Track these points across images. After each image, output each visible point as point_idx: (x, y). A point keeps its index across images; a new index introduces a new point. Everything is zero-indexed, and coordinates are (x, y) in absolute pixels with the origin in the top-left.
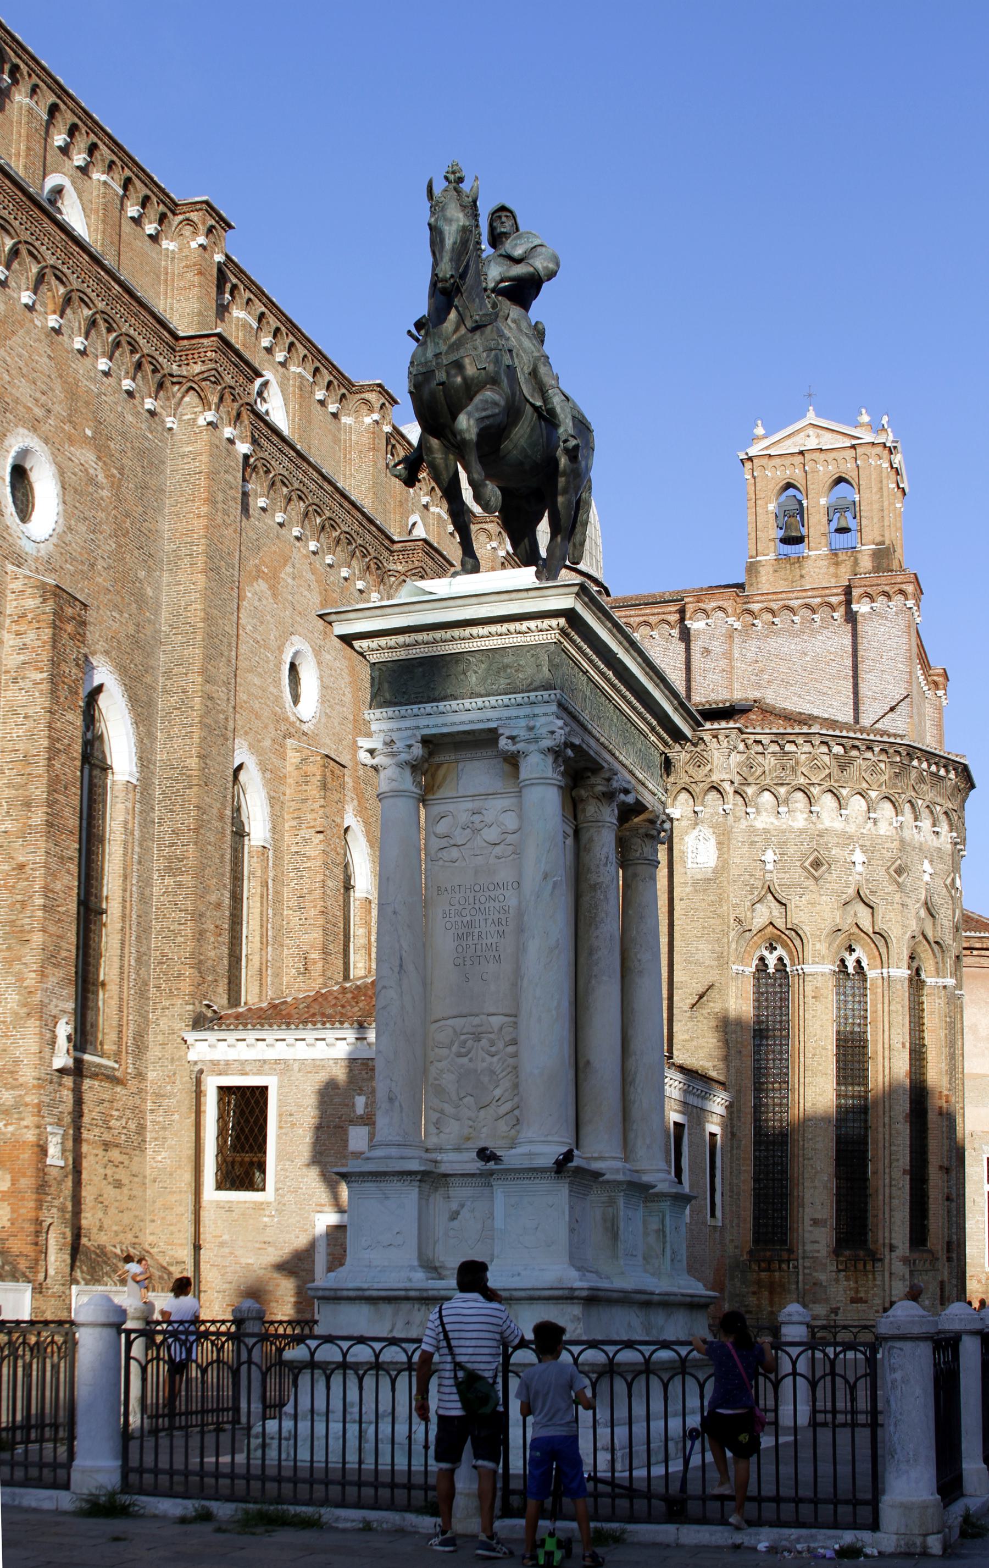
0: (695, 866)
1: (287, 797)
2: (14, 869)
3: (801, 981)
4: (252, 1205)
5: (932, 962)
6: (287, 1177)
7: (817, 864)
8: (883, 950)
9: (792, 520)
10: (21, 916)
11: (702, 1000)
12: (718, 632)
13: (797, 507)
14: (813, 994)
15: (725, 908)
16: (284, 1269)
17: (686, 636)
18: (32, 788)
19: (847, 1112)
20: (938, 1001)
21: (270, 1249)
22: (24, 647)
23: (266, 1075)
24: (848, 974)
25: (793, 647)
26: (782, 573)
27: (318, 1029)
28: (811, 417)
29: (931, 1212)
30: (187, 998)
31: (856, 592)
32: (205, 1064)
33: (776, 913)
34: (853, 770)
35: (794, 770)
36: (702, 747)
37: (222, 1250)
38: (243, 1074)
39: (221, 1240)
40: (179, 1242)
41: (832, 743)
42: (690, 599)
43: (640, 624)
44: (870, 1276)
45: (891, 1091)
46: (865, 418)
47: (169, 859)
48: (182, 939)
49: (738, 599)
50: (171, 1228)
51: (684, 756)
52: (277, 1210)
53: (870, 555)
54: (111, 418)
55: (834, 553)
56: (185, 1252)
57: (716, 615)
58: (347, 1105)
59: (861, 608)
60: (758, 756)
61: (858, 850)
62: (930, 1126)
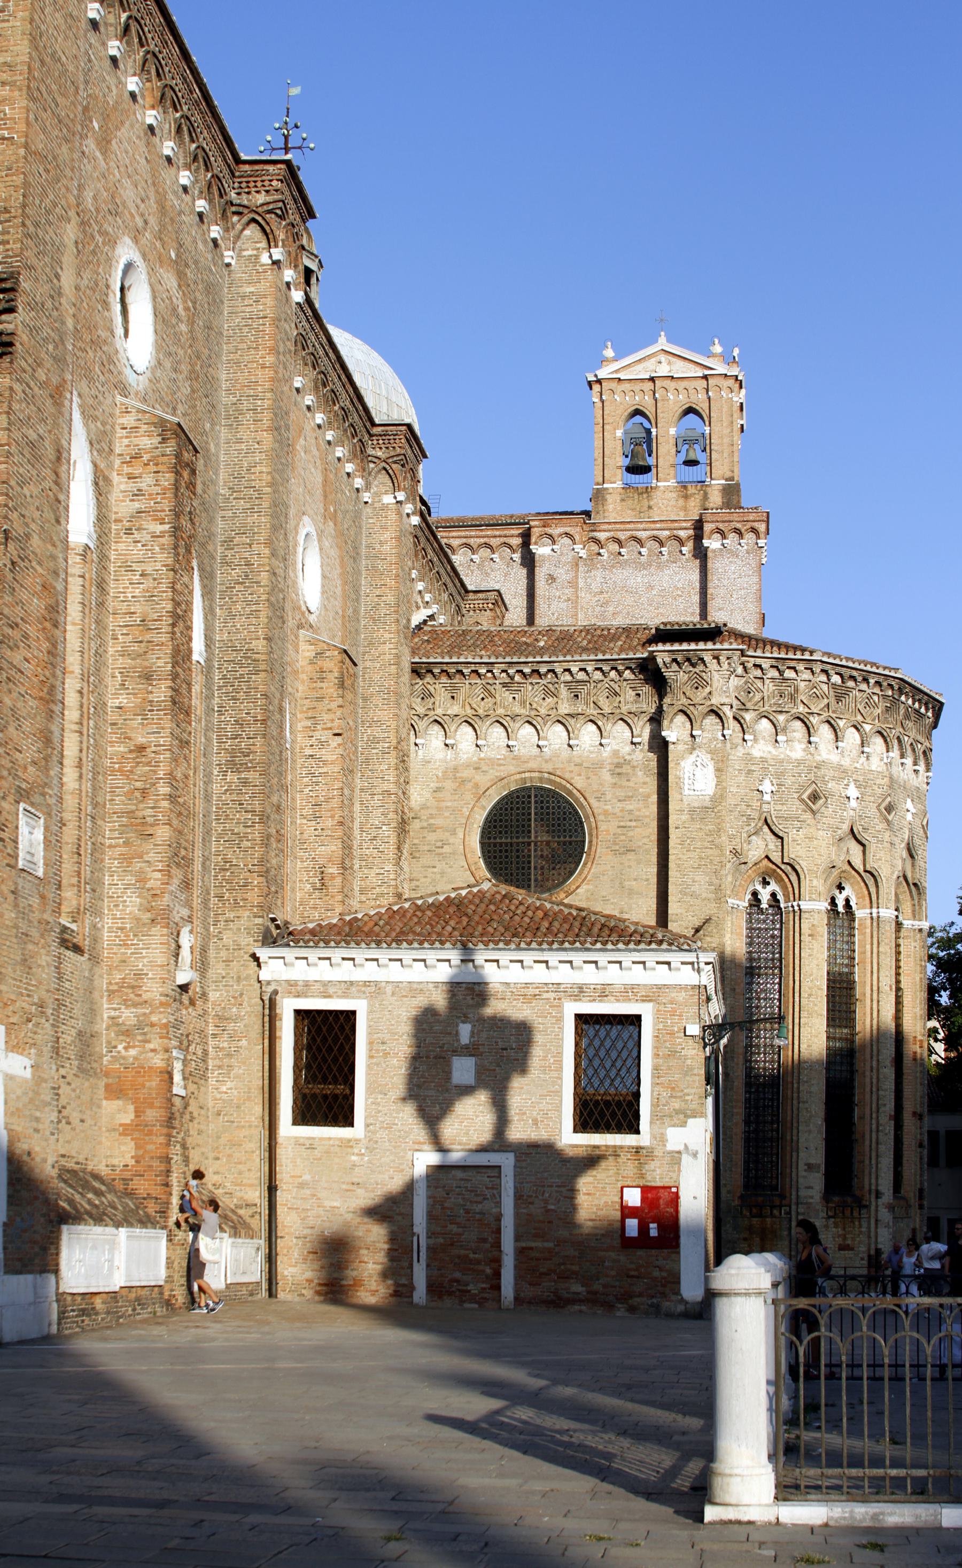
0: (692, 793)
1: (299, 694)
2: (131, 751)
3: (797, 918)
4: (337, 1143)
5: (909, 904)
6: (379, 1112)
7: (815, 797)
8: (873, 890)
9: (639, 448)
10: (142, 806)
11: (698, 934)
12: (563, 559)
13: (644, 435)
14: (810, 932)
15: (724, 838)
16: (375, 1213)
17: (529, 561)
18: (152, 658)
19: (835, 1055)
20: (913, 944)
21: (360, 1191)
22: (139, 493)
23: (353, 998)
24: (838, 913)
25: (639, 580)
26: (630, 502)
27: (414, 949)
28: (662, 342)
29: (905, 1159)
30: (255, 910)
31: (708, 527)
32: (281, 985)
33: (771, 846)
34: (849, 700)
35: (793, 698)
36: (701, 667)
37: (302, 1191)
38: (325, 997)
39: (300, 1180)
40: (249, 1182)
41: (831, 672)
42: (536, 523)
43: (480, 546)
44: (857, 1223)
45: (879, 1036)
46: (718, 349)
47: (232, 753)
48: (249, 844)
49: (584, 526)
50: (240, 1166)
51: (682, 677)
52: (367, 1148)
53: (720, 491)
54: (188, 241)
55: (683, 486)
56: (258, 1194)
57: (562, 541)
58: (450, 1034)
59: (712, 543)
60: (757, 681)
61: (852, 785)
62: (905, 1071)
